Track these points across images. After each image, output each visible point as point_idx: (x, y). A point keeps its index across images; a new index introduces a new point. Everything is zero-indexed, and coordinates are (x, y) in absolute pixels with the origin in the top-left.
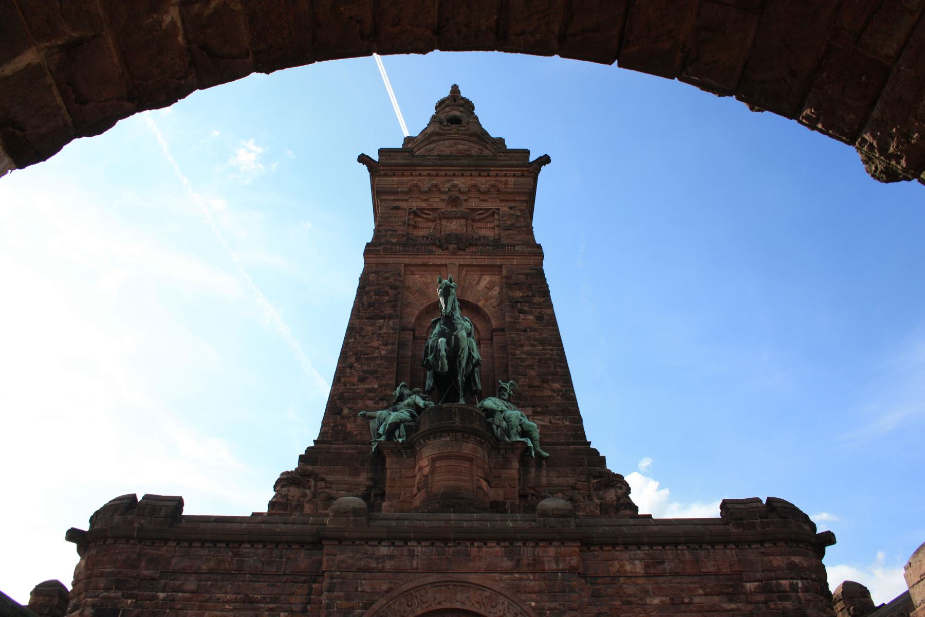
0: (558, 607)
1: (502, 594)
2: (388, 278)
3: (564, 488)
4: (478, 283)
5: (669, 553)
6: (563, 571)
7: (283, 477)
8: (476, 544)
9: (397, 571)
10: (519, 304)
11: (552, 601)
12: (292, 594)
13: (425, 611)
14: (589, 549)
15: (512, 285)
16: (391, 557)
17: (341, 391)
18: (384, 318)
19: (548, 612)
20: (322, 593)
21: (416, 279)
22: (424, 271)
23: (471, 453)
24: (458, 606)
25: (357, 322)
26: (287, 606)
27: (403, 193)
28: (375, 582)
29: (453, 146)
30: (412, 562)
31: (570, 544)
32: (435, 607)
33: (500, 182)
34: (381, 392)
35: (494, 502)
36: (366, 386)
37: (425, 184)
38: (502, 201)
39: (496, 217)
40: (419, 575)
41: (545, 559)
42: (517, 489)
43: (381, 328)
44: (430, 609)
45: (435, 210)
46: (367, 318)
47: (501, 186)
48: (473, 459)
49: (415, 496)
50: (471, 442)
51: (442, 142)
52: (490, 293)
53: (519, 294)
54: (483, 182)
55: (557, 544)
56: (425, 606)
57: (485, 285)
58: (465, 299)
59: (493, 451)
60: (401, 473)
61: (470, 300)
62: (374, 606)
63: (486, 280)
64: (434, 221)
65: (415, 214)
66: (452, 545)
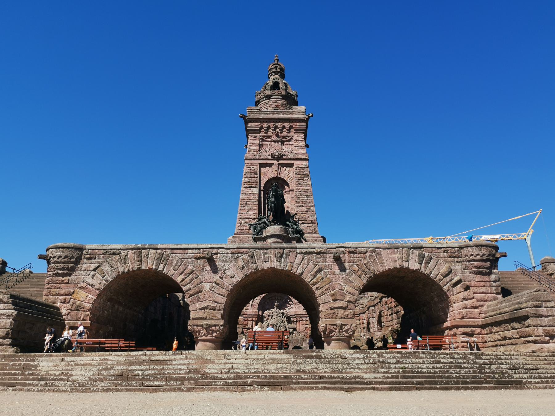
2: (254, 170)
18: (253, 187)
21: (263, 170)
27: (257, 130)
29: (276, 102)
33: (293, 124)
36: (249, 213)
37: (265, 126)
38: (294, 133)
39: (292, 140)
43: (253, 191)
45: (269, 137)
46: (248, 187)
47: (294, 126)
51: (271, 100)
53: (299, 176)
54: (287, 125)
63: (288, 168)
64: (269, 142)
65: (262, 139)
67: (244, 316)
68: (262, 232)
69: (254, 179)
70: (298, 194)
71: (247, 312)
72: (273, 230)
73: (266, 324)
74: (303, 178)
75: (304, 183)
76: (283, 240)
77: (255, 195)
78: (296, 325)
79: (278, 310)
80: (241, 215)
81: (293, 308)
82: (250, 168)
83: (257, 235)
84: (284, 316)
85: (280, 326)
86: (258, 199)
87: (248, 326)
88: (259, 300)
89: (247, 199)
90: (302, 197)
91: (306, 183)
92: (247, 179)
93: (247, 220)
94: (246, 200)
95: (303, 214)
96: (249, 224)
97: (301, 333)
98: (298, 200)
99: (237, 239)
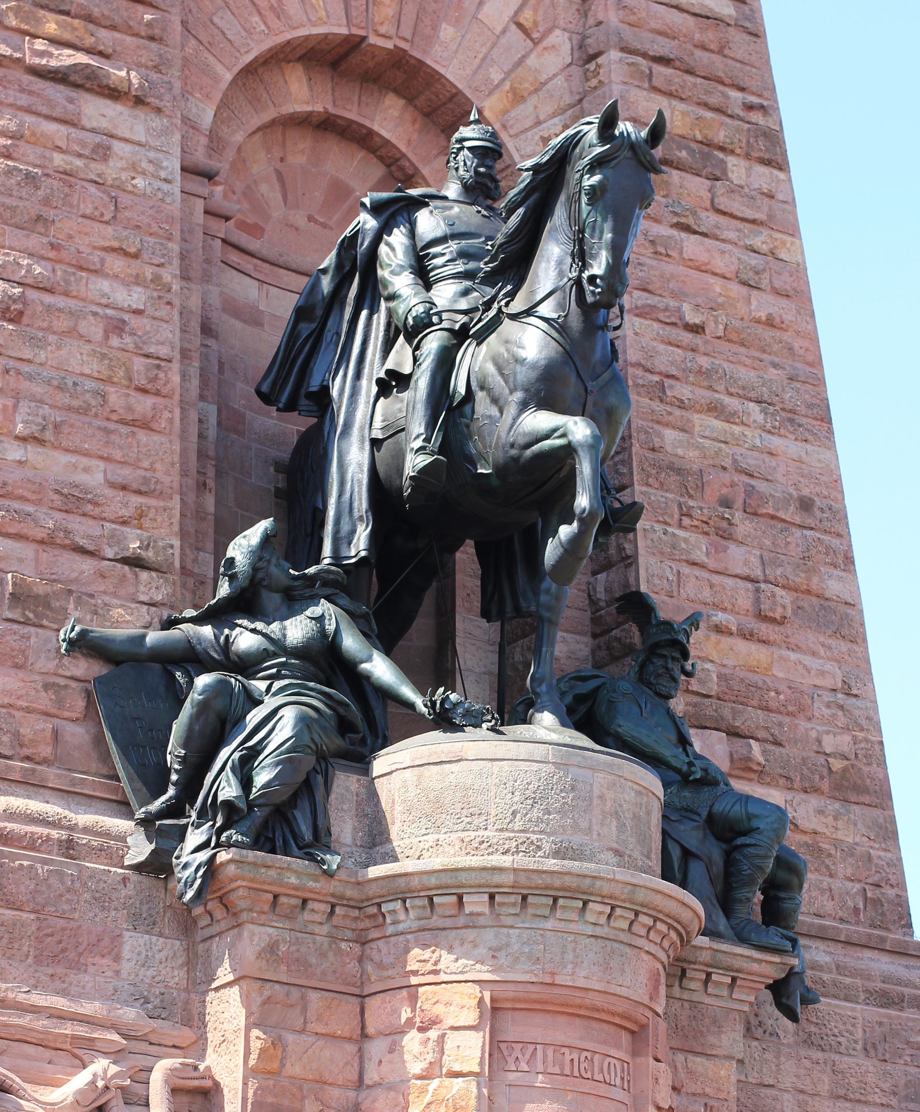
15: (645, 55)
18: (114, 93)
23: (646, 1000)
43: (102, 153)
48: (644, 1027)
57: (511, 13)
58: (429, 62)
60: (304, 1009)
90: (715, 409)
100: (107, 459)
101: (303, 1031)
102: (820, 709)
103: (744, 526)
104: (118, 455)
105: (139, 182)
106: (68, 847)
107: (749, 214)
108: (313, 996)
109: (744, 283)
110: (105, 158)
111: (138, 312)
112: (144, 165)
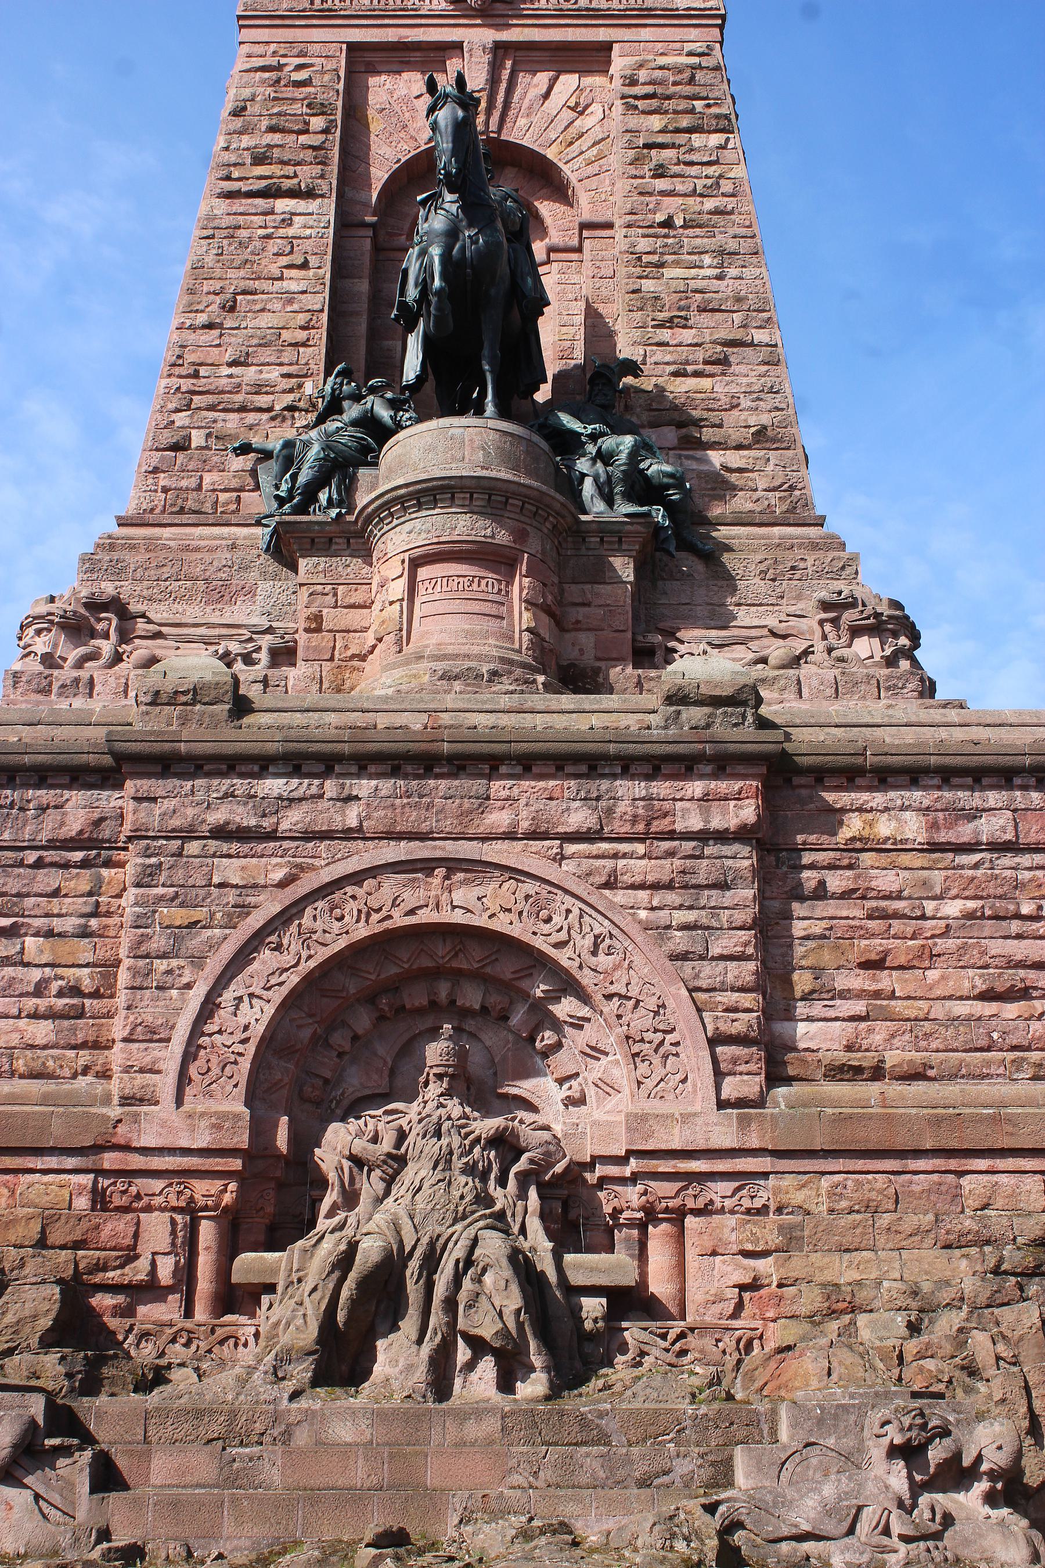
0: (705, 921)
1: (566, 891)
3: (754, 633)
4: (546, 96)
5: (993, 798)
6: (722, 837)
7: (43, 609)
8: (503, 769)
9: (309, 836)
10: (654, 152)
11: (691, 908)
12: (56, 893)
13: (378, 929)
14: (789, 781)
15: (636, 97)
16: (292, 801)
17: (184, 389)
18: (294, 194)
19: (678, 934)
20: (125, 889)
22: (402, 62)
24: (458, 917)
25: (222, 206)
26: (37, 923)
28: (254, 860)
30: (344, 815)
31: (741, 769)
32: (399, 920)
34: (291, 391)
35: (573, 665)
40: (360, 844)
41: (679, 804)
42: (629, 635)
43: (288, 222)
44: (388, 924)
49: (372, 652)
50: (512, 515)
52: (577, 123)
53: (656, 122)
55: (708, 769)
56: (375, 917)
59: (570, 539)
60: (335, 595)
61: (526, 142)
62: (249, 920)
63: (568, 82)
66: (445, 770)
67: (110, 1160)
68: (348, 489)
69: (303, 139)
70: (644, 245)
71: (136, 1118)
72: (431, 449)
73: (327, 1245)
74: (681, 138)
75: (694, 170)
76: (520, 536)
77: (308, 245)
78: (642, 1255)
79: (455, 1108)
80: (186, 384)
81: (606, 1087)
82: (280, 67)
83: (302, 509)
84: (522, 1164)
85: (469, 1262)
86: (326, 272)
87: (143, 1264)
88: (270, 1010)
89: (242, 273)
90: (677, 264)
91: (710, 170)
92: (246, 141)
93: (232, 422)
94: (236, 278)
95: (691, 383)
96: (244, 449)
97: (692, 1341)
98: (648, 285)
99: (133, 559)
100: (281, 364)
101: (336, 607)
102: (745, 402)
103: (695, 318)
104: (286, 361)
105: (308, 232)
106: (234, 546)
107: (705, 159)
108: (341, 587)
109: (701, 195)
110: (290, 225)
111: (304, 292)
112: (311, 223)
